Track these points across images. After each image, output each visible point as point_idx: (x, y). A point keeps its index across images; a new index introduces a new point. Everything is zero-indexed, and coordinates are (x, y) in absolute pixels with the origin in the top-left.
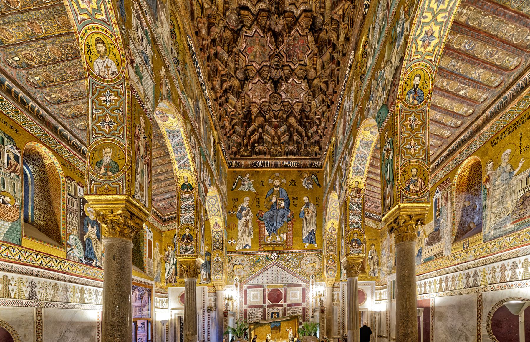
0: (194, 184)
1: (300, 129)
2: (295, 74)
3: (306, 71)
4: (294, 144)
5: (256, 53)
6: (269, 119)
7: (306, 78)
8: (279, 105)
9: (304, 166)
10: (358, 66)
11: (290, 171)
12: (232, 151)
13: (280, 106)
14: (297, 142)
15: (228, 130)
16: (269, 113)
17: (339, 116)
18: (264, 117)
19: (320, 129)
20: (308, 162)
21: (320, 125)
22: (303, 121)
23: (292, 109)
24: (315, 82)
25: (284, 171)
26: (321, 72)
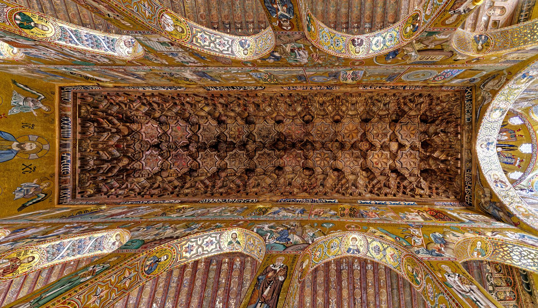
2: (164, 161)
3: (167, 169)
4: (97, 165)
5: (177, 132)
6: (126, 139)
7: (162, 170)
8: (140, 149)
10: (171, 208)
11: (54, 164)
12: (87, 96)
13: (139, 150)
14: (99, 169)
15: (114, 98)
16: (132, 140)
17: (130, 206)
18: (128, 135)
19: (115, 190)
20: (70, 186)
21: (120, 190)
22: (124, 172)
23: (136, 161)
24: (159, 178)
25: (54, 156)
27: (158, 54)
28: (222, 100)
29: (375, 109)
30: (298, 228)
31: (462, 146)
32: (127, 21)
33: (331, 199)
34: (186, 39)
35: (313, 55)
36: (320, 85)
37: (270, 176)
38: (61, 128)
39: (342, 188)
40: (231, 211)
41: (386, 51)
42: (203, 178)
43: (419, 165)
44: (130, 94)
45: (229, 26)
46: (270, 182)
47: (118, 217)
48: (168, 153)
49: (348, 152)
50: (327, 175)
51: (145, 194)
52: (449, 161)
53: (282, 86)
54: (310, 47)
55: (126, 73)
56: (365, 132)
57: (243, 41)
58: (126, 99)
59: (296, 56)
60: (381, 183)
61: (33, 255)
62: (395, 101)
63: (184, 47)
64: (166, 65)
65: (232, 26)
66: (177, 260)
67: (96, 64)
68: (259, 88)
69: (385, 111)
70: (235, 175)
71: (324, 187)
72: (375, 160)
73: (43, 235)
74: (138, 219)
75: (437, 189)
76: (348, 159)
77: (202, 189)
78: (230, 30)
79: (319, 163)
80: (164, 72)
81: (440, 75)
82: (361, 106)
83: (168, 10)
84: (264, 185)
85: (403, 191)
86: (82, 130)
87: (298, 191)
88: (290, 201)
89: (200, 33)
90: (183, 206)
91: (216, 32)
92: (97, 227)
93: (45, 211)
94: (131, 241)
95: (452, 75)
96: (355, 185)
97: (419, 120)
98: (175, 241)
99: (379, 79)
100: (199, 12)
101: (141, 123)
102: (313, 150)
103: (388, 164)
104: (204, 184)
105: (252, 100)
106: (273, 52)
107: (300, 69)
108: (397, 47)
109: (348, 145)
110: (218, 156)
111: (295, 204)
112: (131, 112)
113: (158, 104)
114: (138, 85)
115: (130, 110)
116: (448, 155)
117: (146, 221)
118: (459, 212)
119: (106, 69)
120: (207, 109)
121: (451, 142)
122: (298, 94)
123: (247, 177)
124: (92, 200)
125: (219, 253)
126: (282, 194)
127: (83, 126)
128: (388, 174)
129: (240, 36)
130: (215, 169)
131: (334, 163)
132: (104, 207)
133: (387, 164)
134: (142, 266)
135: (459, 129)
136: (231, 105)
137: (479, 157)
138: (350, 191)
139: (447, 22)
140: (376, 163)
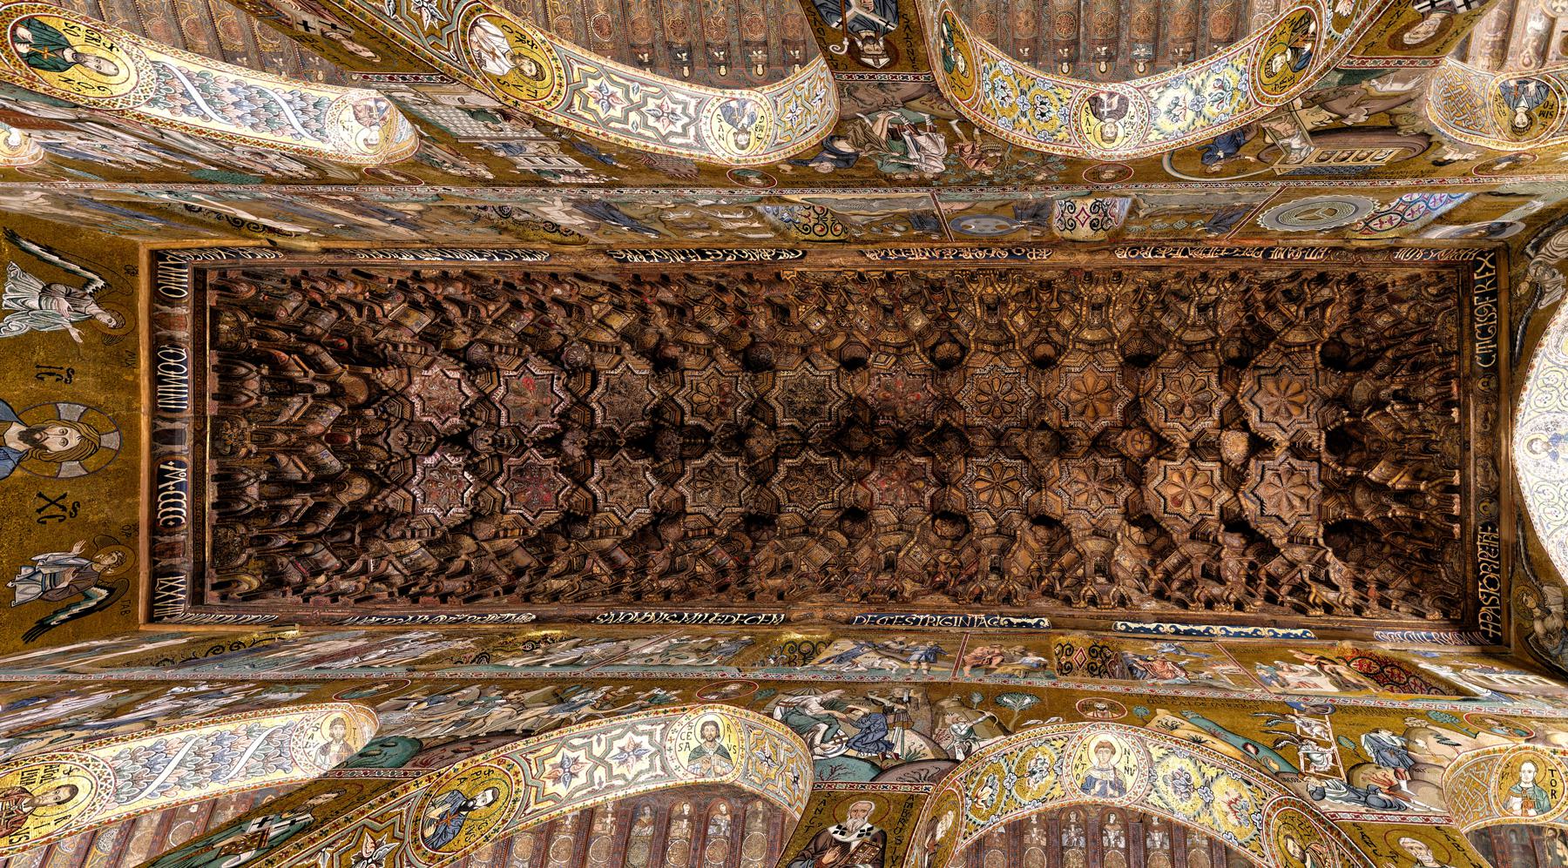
0: (64, 86)
1: (330, 516)
2: (484, 489)
3: (491, 514)
4: (269, 499)
6: (361, 417)
7: (476, 515)
10: (505, 640)
11: (136, 493)
12: (237, 281)
13: (401, 451)
14: (275, 511)
15: (322, 286)
16: (380, 418)
18: (367, 405)
19: (329, 579)
20: (185, 563)
21: (343, 578)
22: (355, 523)
23: (394, 487)
24: (467, 542)
26: (490, 550)
27: (465, 148)
28: (666, 295)
29: (1168, 322)
30: (917, 707)
31: (1465, 446)
32: (361, 44)
34: (549, 99)
35: (962, 149)
37: (824, 540)
38: (156, 380)
39: (1061, 579)
40: (698, 651)
41: (1204, 136)
42: (607, 542)
43: (1320, 506)
44: (373, 272)
45: (688, 57)
47: (338, 664)
48: (496, 463)
49: (1081, 463)
50: (1013, 538)
51: (423, 593)
52: (1423, 495)
53: (861, 247)
54: (954, 123)
55: (360, 207)
56: (1137, 397)
57: (734, 104)
58: (359, 289)
59: (906, 153)
60: (1191, 567)
61: (73, 781)
62: (1236, 297)
63: (545, 124)
64: (487, 183)
65: (699, 56)
66: (527, 806)
67: (266, 180)
69: (1203, 328)
70: (711, 534)
71: (1002, 577)
72: (1171, 491)
73: (103, 718)
74: (401, 673)
75: (1382, 586)
77: (605, 578)
78: (691, 70)
79: (984, 497)
80: (481, 205)
81: (1386, 213)
82: (1123, 314)
83: (494, 7)
84: (804, 568)
85: (1269, 592)
86: (222, 387)
87: (918, 587)
89: (595, 78)
90: (544, 632)
91: (646, 75)
92: (272, 696)
93: (107, 642)
94: (381, 742)
95: (1428, 210)
96: (1105, 569)
97: (1318, 360)
98: (521, 744)
99: (1181, 224)
100: (592, 13)
101: (409, 368)
102: (966, 456)
103: (1216, 505)
104: (612, 562)
105: (764, 294)
106: (832, 138)
107: (919, 194)
108: (1241, 121)
109: (1081, 441)
110: (657, 473)
111: (907, 631)
112: (376, 332)
113: (463, 306)
114: (398, 247)
115: (371, 325)
116: (1417, 476)
117: (425, 680)
118: (1457, 663)
119: (296, 194)
120: (618, 322)
121: (1426, 432)
122: (913, 274)
123: (749, 542)
124: (254, 610)
125: (662, 785)
126: (864, 596)
127: (226, 373)
128: (1215, 539)
129: (723, 87)
130: (643, 514)
131: (1035, 499)
132: (292, 633)
133: (1211, 502)
134: (416, 821)
135: (1455, 389)
136: (697, 309)
137: (1523, 484)
138: (1088, 590)
139: (1408, 38)
140: (1174, 498)
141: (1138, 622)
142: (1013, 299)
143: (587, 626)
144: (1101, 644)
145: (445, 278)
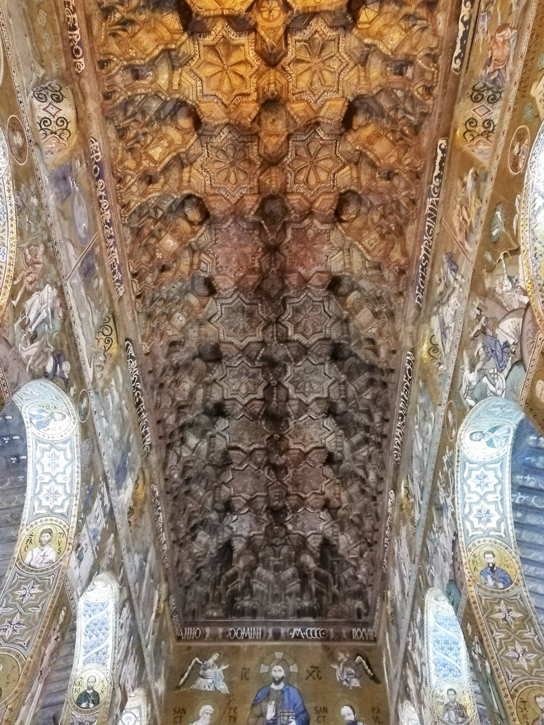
9: (337, 637)
28: (171, 419)
33: (435, 158)
36: (95, 203)
37: (355, 311)
46: (369, 312)
53: (116, 303)
68: (131, 352)
76: (315, 78)
79: (323, 176)
87: (397, 246)
88: (423, 278)
104: (359, 444)
110: (298, 415)
122: (130, 256)
131: (327, 129)
136: (178, 399)
138: (418, 90)
141: (455, 43)
142: (139, 164)
143: (402, 467)
144: (470, 92)
145: (175, 530)
